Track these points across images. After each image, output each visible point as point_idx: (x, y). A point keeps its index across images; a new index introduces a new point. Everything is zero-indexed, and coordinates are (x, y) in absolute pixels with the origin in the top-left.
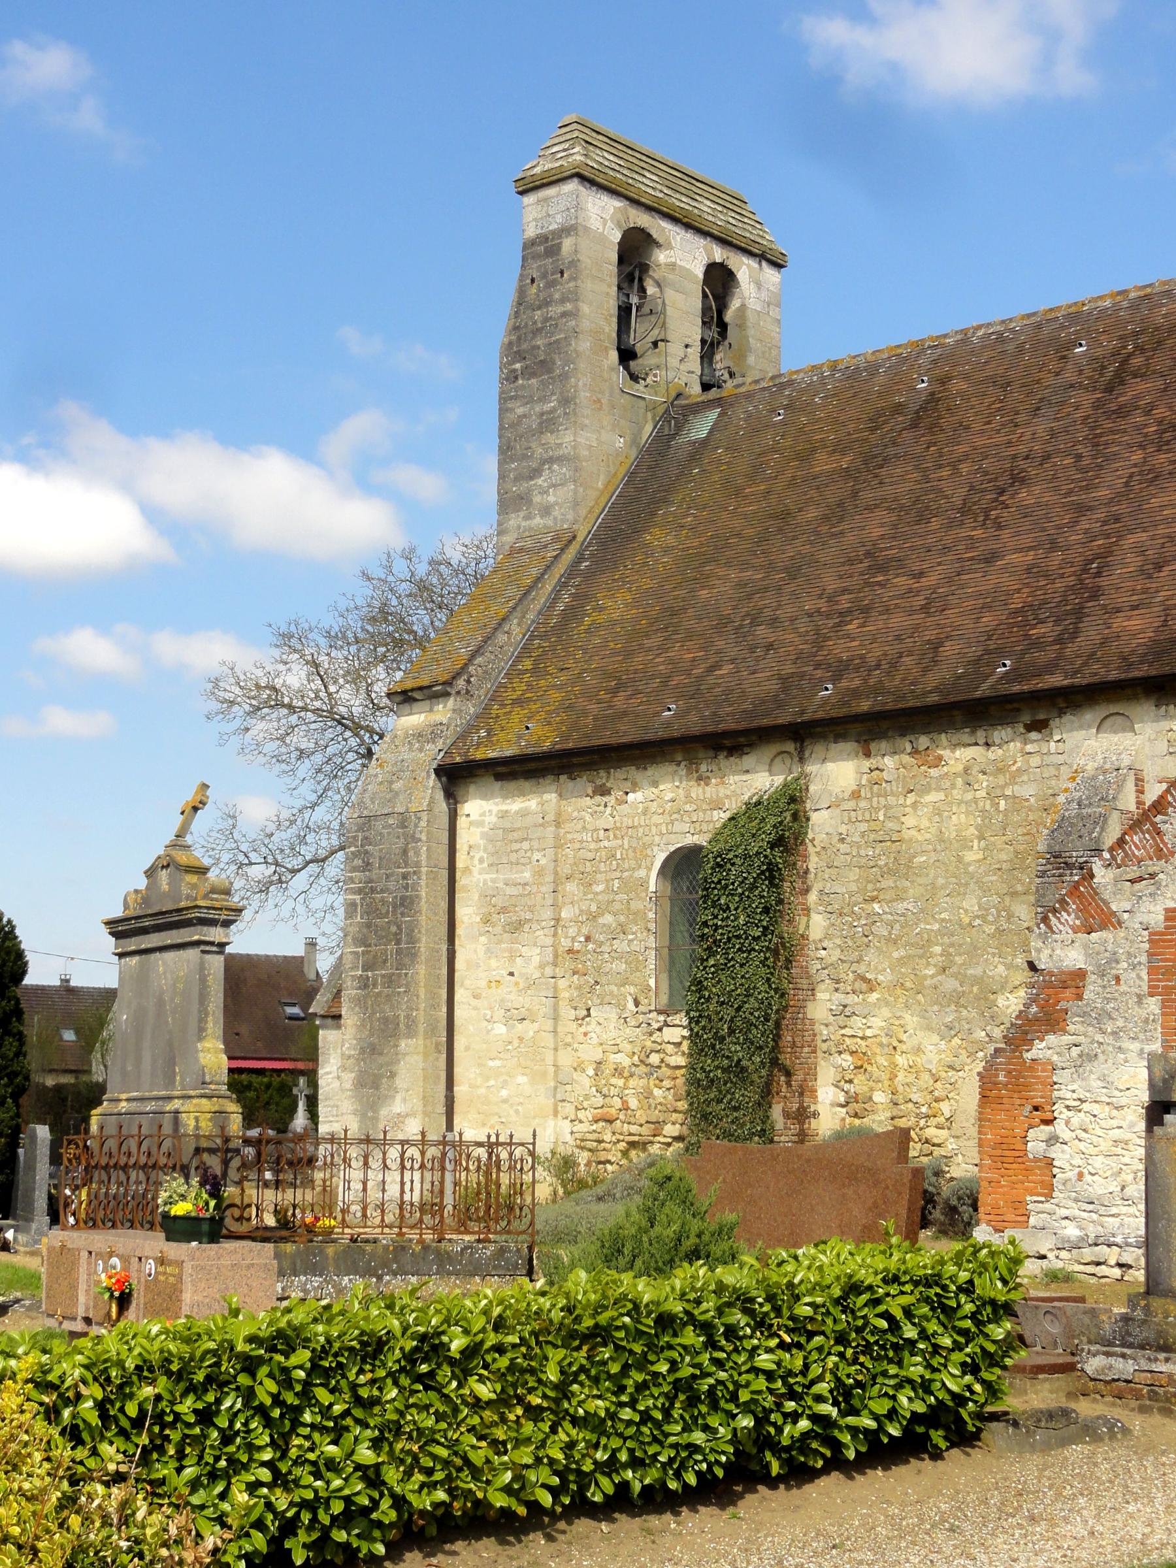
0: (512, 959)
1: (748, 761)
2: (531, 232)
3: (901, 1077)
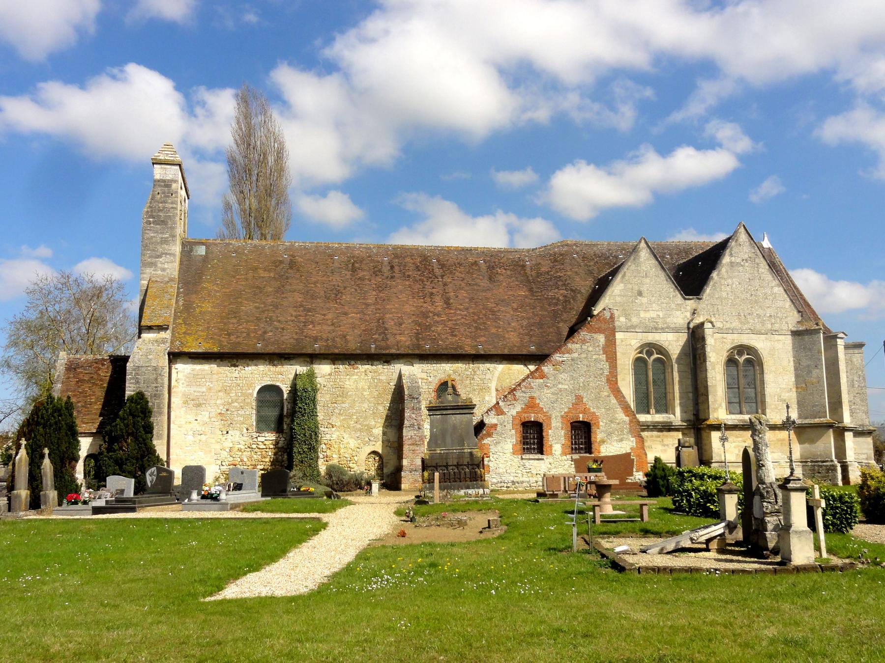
0: (196, 415)
1: (292, 362)
2: (157, 177)
3: (342, 451)
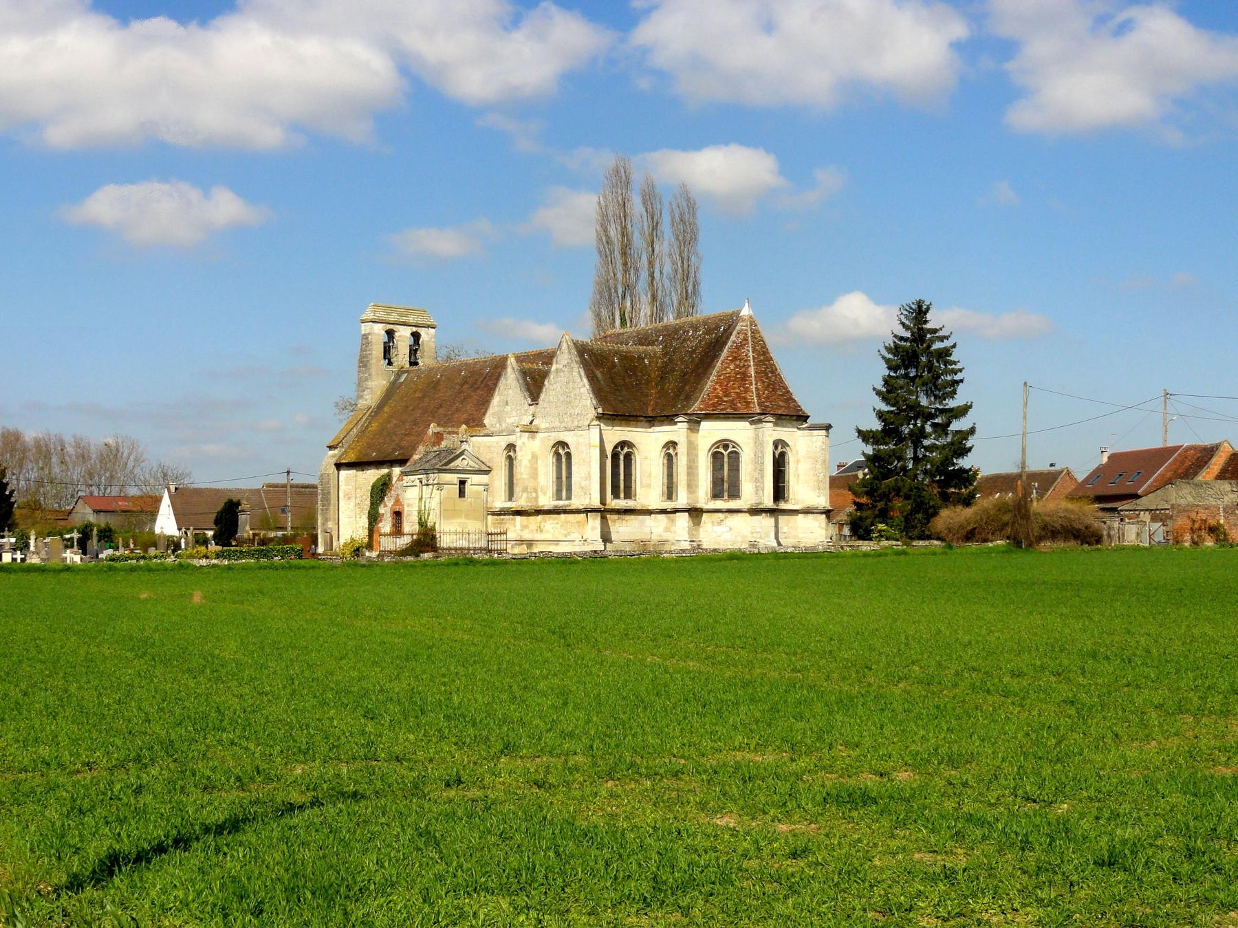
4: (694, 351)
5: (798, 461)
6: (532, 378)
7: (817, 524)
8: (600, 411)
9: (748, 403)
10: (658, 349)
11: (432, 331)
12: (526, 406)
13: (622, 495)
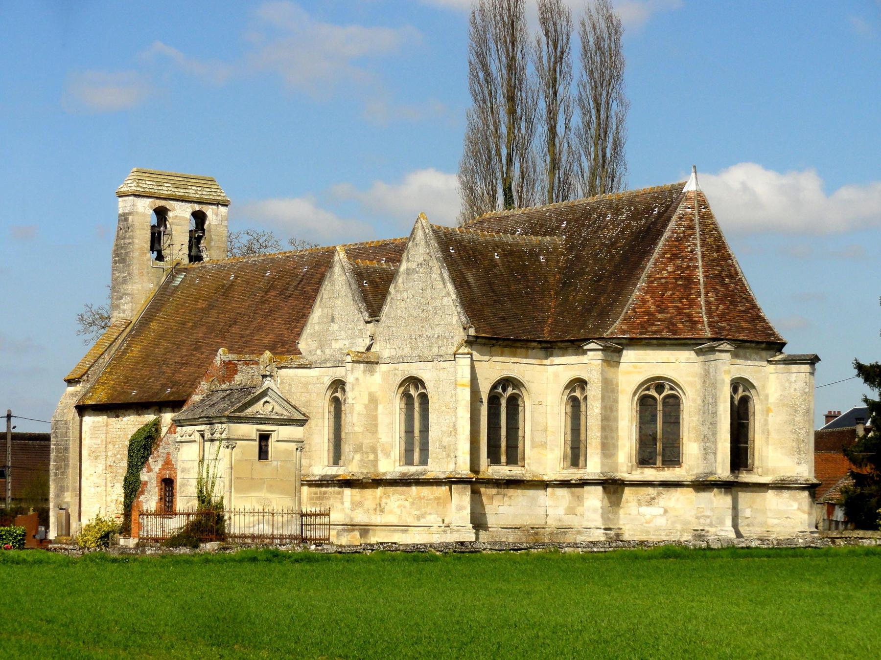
1: (149, 411)
2: (121, 211)
4: (613, 244)
5: (768, 411)
6: (371, 282)
7: (795, 505)
8: (472, 332)
9: (693, 323)
10: (560, 240)
11: (223, 210)
12: (362, 322)
13: (503, 459)
